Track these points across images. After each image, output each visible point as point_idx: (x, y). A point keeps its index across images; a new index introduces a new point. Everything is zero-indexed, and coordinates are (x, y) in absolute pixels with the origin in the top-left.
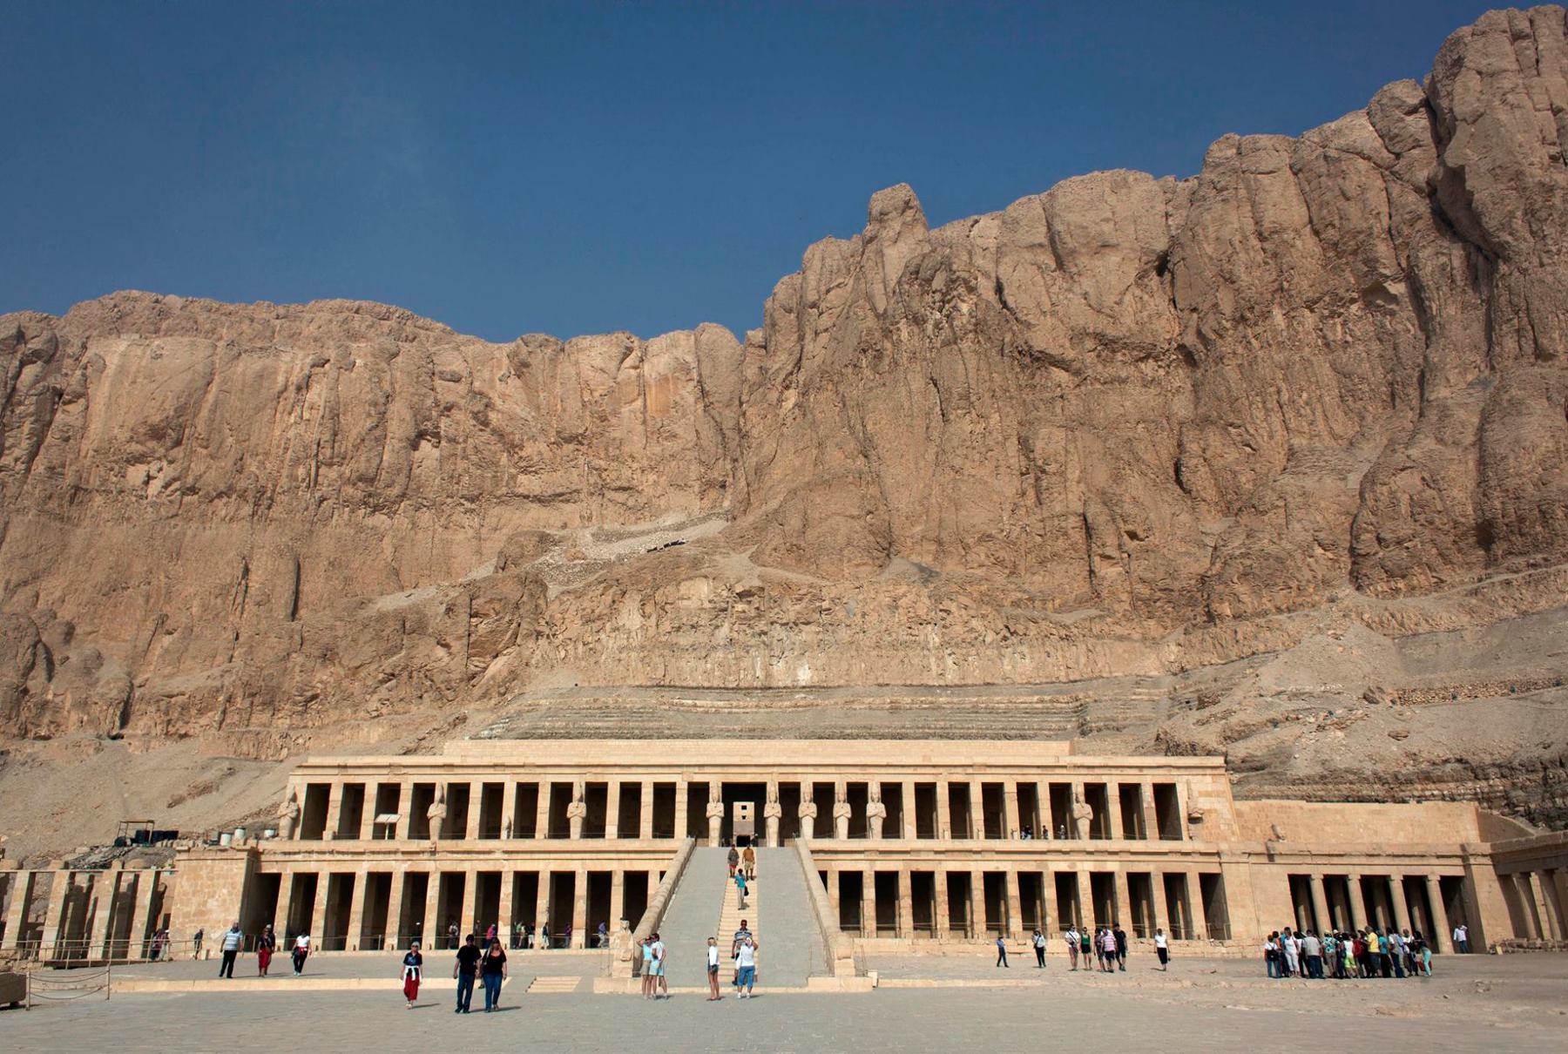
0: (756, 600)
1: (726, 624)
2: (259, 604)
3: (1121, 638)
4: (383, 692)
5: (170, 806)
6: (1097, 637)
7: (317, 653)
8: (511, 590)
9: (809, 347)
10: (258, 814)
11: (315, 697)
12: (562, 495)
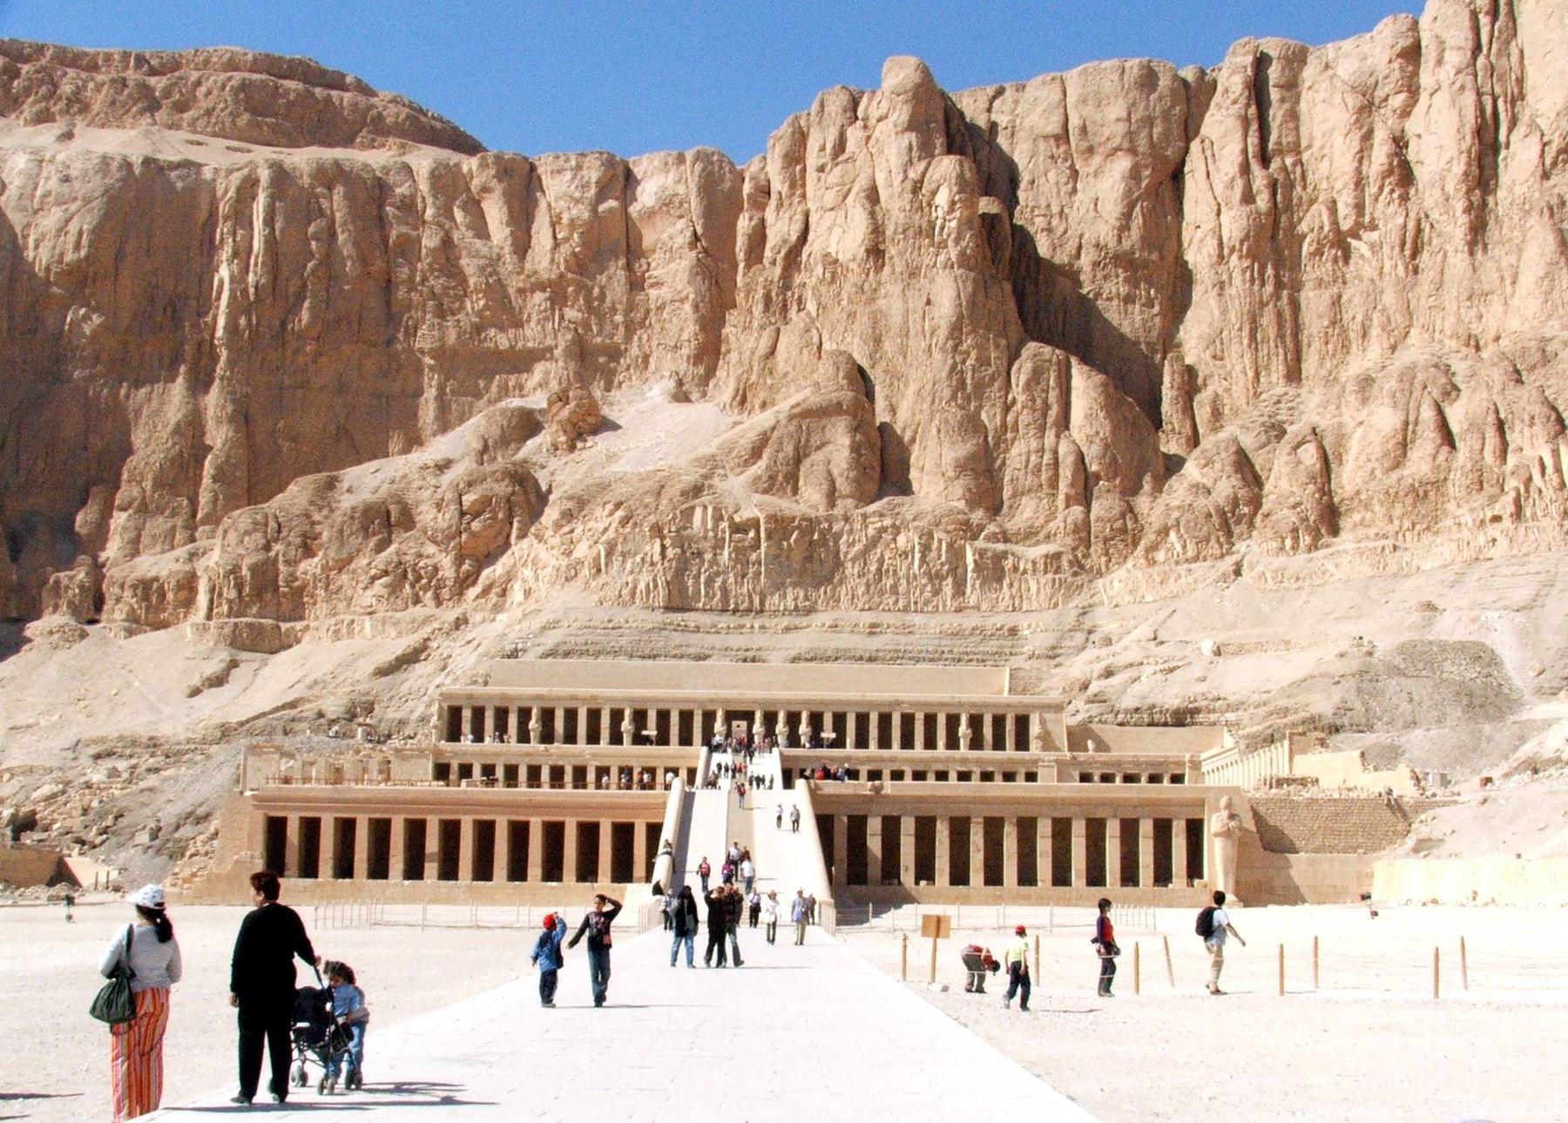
0: (752, 534)
1: (726, 552)
2: (215, 479)
3: (1075, 574)
4: (379, 587)
6: (1056, 572)
7: (298, 540)
8: (502, 488)
9: (813, 219)
10: (283, 707)
11: (302, 589)
12: (531, 351)
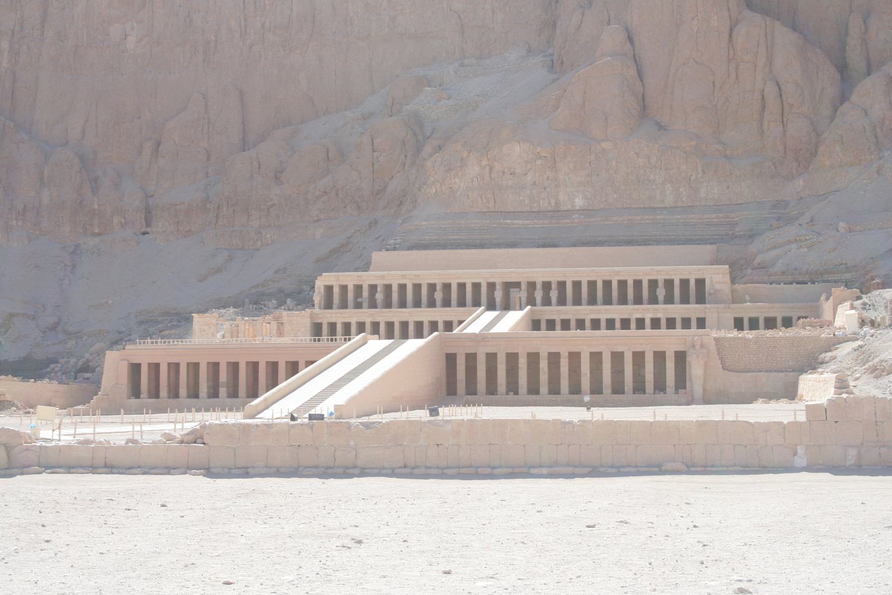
5: (200, 281)
10: (258, 286)
